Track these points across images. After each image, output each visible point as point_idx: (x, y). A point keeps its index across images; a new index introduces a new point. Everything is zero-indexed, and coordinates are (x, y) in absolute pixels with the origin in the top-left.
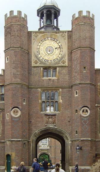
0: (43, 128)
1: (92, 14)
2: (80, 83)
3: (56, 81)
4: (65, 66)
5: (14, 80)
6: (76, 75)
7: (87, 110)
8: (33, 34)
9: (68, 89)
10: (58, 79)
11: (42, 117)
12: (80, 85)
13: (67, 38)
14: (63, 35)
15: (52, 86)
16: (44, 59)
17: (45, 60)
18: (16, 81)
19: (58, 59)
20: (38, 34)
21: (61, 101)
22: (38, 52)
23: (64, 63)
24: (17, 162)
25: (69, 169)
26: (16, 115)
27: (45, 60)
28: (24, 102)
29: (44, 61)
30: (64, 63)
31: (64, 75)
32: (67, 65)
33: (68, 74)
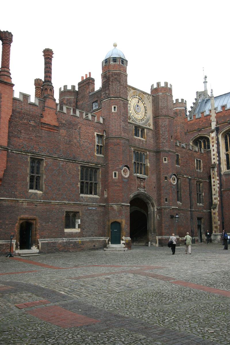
0: (136, 192)
1: (170, 84)
2: (169, 151)
3: (145, 142)
4: (151, 129)
5: (123, 134)
6: (165, 141)
7: (175, 179)
9: (153, 153)
10: (146, 141)
11: (135, 180)
12: (170, 153)
15: (142, 147)
18: (125, 136)
21: (148, 165)
24: (127, 231)
25: (156, 240)
30: (149, 126)
31: (150, 137)
33: (153, 138)
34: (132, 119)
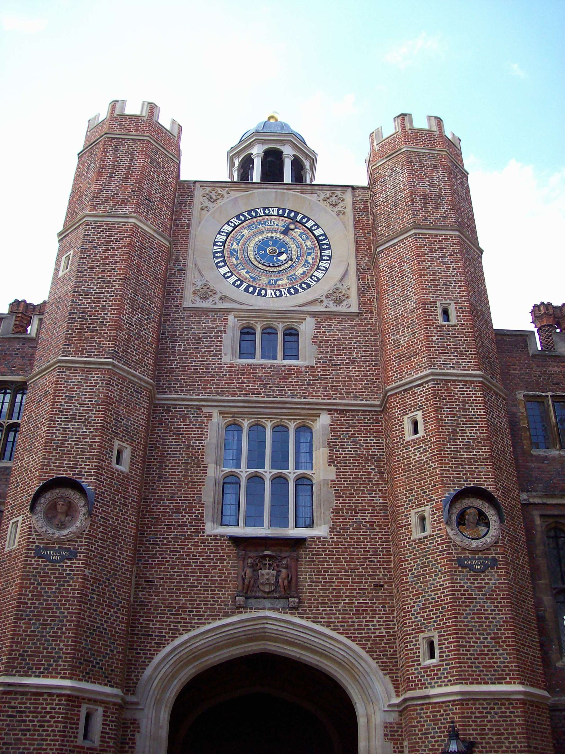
7: (481, 514)
8: (198, 193)
13: (349, 210)
14: (334, 200)
16: (245, 285)
17: (251, 289)
19: (309, 286)
20: (224, 193)
22: (219, 255)
23: (338, 302)
26: (62, 526)
27: (251, 289)
28: (118, 463)
29: (246, 290)
30: (338, 302)
32: (355, 309)
34: (218, 296)
